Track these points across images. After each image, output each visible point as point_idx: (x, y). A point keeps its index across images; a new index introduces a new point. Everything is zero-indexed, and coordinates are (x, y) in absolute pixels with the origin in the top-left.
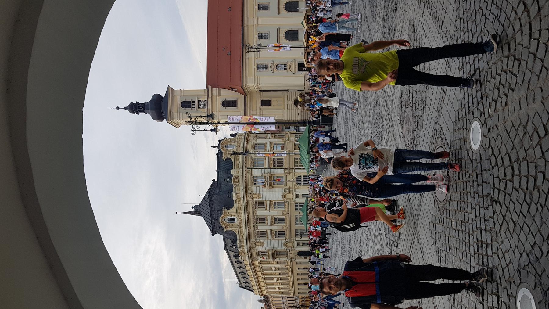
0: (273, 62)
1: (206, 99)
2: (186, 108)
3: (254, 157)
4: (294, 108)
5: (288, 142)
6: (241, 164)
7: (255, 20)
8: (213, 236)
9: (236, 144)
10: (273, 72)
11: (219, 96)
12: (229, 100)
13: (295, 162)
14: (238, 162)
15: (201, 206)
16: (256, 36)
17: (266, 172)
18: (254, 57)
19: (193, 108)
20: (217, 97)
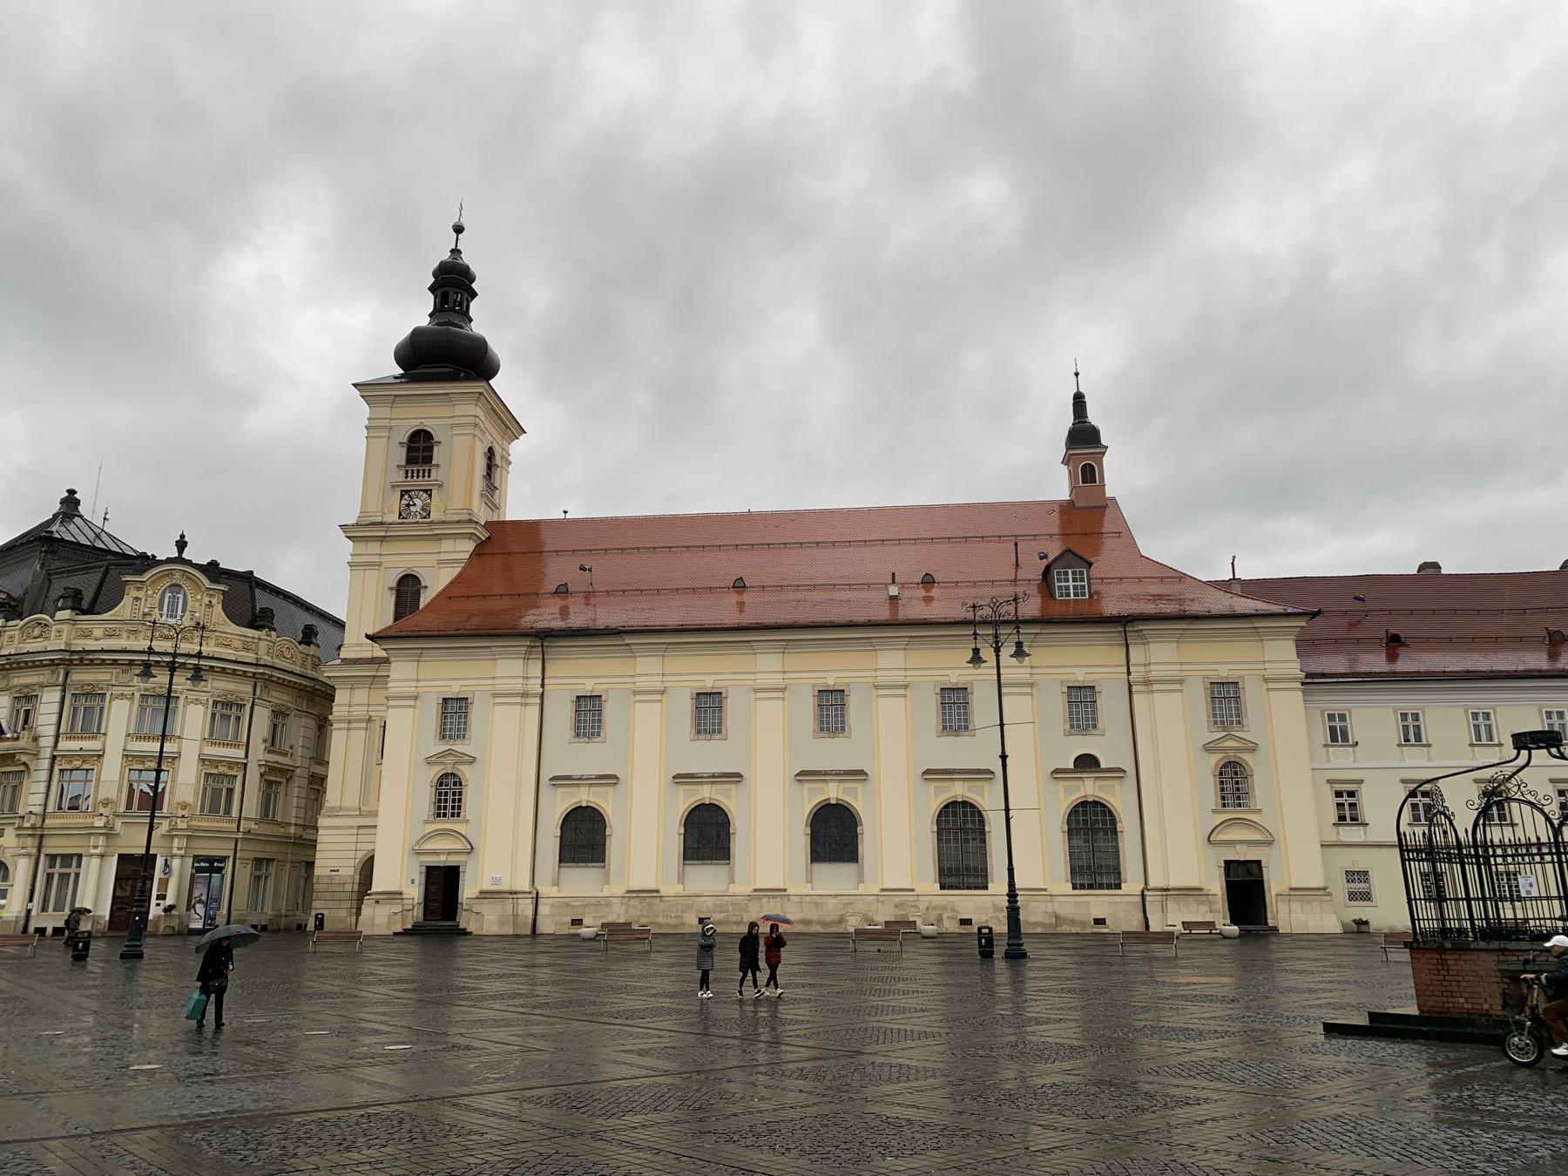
0: (473, 760)
1: (433, 517)
2: (409, 450)
3: (108, 696)
6: (91, 644)
7: (654, 682)
10: (429, 762)
11: (440, 562)
13: (71, 856)
16: (589, 687)
18: (497, 681)
19: (402, 473)
20: (436, 557)
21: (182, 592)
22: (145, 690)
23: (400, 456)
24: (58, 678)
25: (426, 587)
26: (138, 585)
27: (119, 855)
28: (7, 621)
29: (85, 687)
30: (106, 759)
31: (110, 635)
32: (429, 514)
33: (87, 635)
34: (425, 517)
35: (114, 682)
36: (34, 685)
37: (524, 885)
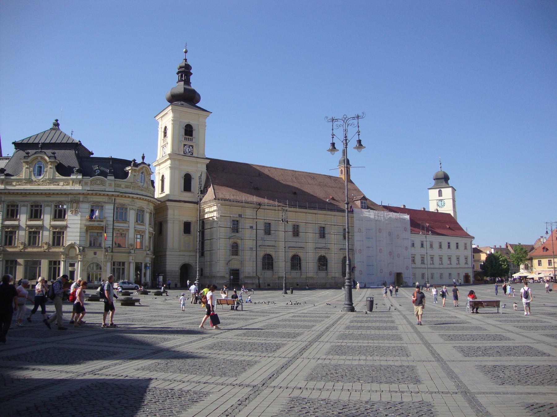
1: (195, 155)
3: (128, 209)
4: (180, 264)
5: (145, 254)
8: (13, 143)
9: (145, 185)
12: (192, 183)
14: (123, 186)
15: (58, 132)
17: (109, 223)
22: (138, 208)
23: (183, 132)
24: (112, 201)
25: (193, 179)
26: (135, 171)
27: (136, 263)
28: (83, 176)
31: (127, 187)
32: (193, 154)
33: (119, 186)
34: (191, 155)
36: (101, 202)
37: (254, 275)
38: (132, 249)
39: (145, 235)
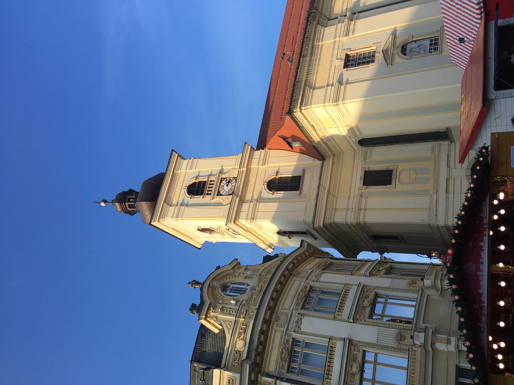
21: (229, 285)
22: (298, 305)
23: (198, 199)
29: (284, 355)
30: (356, 338)
32: (234, 178)
34: (236, 180)
35: (285, 329)
38: (412, 337)
39: (375, 288)
